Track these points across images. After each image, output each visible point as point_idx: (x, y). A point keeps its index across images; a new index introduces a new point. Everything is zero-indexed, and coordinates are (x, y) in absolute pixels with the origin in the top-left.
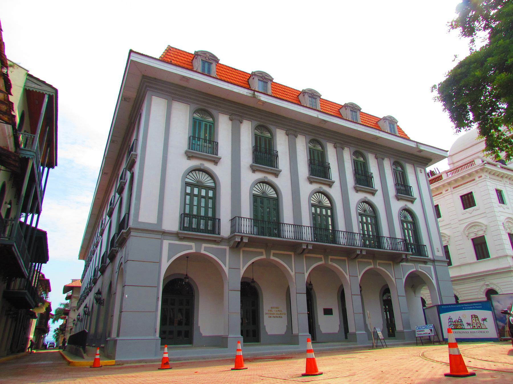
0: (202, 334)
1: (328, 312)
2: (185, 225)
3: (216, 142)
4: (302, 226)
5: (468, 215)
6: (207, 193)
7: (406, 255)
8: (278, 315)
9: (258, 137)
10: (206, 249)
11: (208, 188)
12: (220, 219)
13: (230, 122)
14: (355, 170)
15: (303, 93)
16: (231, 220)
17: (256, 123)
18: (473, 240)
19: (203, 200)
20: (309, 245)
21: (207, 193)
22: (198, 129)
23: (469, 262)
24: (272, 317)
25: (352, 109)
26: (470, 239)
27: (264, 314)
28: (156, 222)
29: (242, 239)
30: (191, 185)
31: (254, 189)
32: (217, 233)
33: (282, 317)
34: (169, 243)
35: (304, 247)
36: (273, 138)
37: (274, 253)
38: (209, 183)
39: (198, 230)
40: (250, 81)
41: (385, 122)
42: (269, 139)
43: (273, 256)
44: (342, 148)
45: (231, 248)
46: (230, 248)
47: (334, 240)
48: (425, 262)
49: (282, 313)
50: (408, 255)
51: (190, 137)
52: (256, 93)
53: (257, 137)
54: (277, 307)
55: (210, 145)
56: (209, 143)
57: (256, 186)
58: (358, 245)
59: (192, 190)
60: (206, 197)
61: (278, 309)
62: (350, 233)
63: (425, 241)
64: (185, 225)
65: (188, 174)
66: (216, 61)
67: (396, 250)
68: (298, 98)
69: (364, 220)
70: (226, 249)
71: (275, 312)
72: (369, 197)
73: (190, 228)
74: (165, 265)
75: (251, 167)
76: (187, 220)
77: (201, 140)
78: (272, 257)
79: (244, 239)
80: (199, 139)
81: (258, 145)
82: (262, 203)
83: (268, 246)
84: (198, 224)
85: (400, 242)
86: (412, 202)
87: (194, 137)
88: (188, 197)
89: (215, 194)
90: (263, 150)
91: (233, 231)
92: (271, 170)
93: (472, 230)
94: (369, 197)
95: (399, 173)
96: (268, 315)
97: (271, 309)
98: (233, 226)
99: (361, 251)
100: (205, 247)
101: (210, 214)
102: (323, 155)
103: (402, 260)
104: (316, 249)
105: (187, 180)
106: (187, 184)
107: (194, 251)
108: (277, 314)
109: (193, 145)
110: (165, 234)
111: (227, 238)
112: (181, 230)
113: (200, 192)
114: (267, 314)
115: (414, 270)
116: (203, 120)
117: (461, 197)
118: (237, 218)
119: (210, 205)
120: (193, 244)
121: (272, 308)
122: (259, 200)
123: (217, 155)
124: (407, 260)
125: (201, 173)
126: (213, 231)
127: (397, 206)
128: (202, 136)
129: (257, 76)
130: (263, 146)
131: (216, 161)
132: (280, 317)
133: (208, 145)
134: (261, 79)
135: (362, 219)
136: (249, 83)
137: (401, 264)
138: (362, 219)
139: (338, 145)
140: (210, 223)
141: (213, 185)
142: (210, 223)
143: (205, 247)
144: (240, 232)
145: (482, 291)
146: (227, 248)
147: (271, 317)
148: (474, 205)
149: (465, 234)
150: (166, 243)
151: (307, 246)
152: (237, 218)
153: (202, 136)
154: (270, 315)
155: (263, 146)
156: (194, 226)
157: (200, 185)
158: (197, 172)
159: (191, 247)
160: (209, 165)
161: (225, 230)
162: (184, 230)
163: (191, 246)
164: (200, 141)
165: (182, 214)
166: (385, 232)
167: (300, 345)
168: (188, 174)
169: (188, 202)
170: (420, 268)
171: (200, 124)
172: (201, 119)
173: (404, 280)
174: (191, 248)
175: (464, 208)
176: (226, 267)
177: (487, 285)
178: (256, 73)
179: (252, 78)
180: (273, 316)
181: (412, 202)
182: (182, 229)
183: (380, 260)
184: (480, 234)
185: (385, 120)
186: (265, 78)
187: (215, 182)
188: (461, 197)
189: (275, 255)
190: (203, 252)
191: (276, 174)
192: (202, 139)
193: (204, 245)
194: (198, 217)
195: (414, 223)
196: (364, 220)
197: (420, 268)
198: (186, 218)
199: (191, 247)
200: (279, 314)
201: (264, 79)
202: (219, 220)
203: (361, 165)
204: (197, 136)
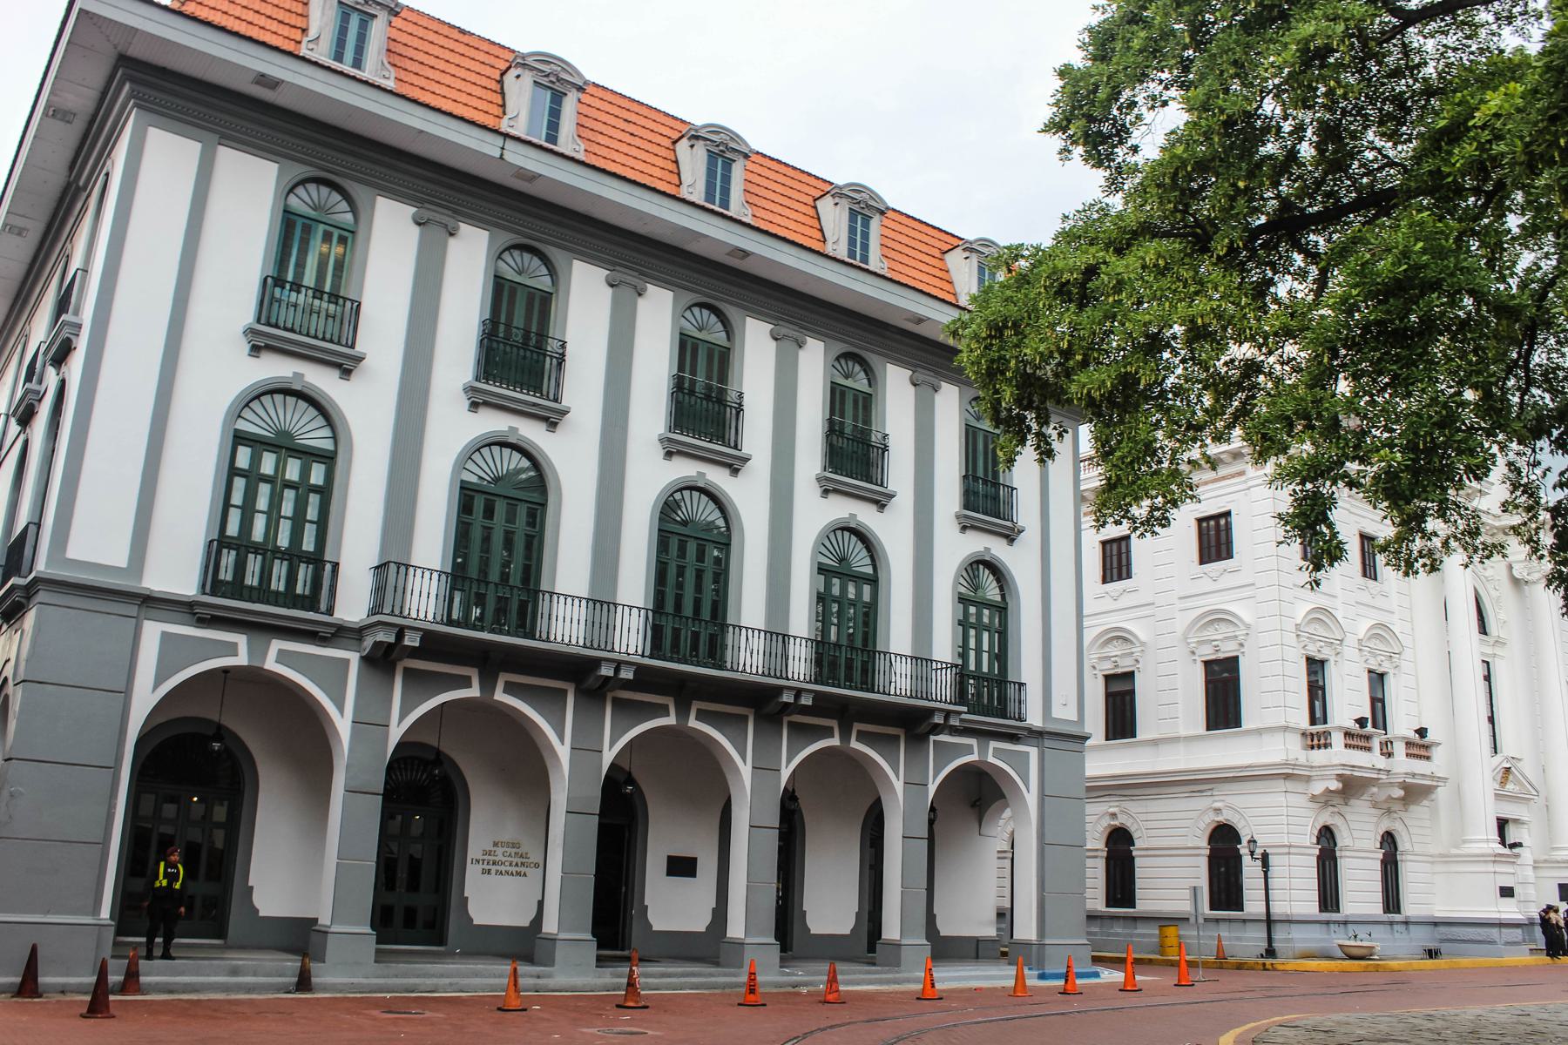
0: (258, 911)
1: (682, 867)
2: (222, 576)
3: (353, 301)
4: (615, 604)
5: (1207, 584)
6: (305, 472)
7: (948, 714)
8: (514, 869)
9: (507, 285)
10: (283, 657)
11: (310, 455)
12: (338, 564)
13: (415, 231)
14: (831, 422)
15: (689, 139)
16: (377, 568)
17: (507, 238)
18: (1207, 663)
19: (289, 495)
20: (623, 666)
21: (305, 472)
22: (299, 250)
23: (1183, 732)
24: (493, 872)
25: (856, 207)
26: (1199, 660)
27: (469, 861)
28: (124, 564)
29: (400, 635)
30: (251, 443)
31: (470, 465)
32: (323, 607)
33: (525, 875)
34: (165, 635)
35: (606, 671)
36: (557, 291)
37: (507, 683)
38: (315, 436)
39: (263, 593)
40: (509, 78)
41: (966, 258)
42: (544, 294)
43: (505, 691)
44: (796, 340)
45: (367, 660)
46: (362, 658)
48: (1013, 738)
49: (530, 861)
50: (952, 715)
51: (265, 280)
52: (510, 144)
53: (503, 285)
54: (513, 844)
55: (332, 307)
56: (329, 302)
57: (477, 457)
58: (790, 676)
59: (256, 460)
60: (303, 488)
61: (514, 850)
62: (777, 634)
63: (1027, 668)
64: (222, 576)
65: (239, 416)
66: (392, 9)
67: (922, 698)
68: (674, 151)
69: (836, 591)
70: (347, 662)
71: (504, 859)
72: (865, 515)
73: (237, 588)
75: (470, 390)
76: (229, 559)
77: (303, 290)
78: (500, 696)
79: (406, 637)
80: (297, 286)
81: (503, 319)
82: (489, 512)
83: (490, 661)
84: (266, 574)
85: (942, 669)
86: (1011, 540)
87: (279, 282)
88: (239, 484)
89: (329, 476)
90: (518, 336)
91: (376, 609)
92: (534, 405)
93: (1210, 633)
94: (865, 515)
96: (480, 867)
97: (493, 849)
98: (379, 590)
99: (799, 693)
100: (280, 651)
101: (308, 545)
102: (722, 360)
103: (936, 729)
104: (646, 679)
105: (242, 425)
106: (240, 438)
107: (245, 663)
108: (511, 865)
109: (276, 305)
111: (357, 626)
112: (204, 593)
113: (280, 467)
114: (478, 861)
115: (974, 757)
116: (319, 219)
117: (1200, 521)
118: (393, 567)
119: (312, 513)
120: (241, 640)
121: (496, 844)
122: (479, 504)
123: (353, 347)
124: (954, 731)
125: (291, 400)
126: (311, 602)
128: (309, 279)
129: (532, 69)
130: (519, 321)
131: (346, 366)
132: (518, 874)
133: (325, 305)
134: (544, 81)
135: (828, 585)
136: (502, 88)
137: (932, 738)
138: (828, 585)
139: (784, 331)
140: (304, 573)
141: (327, 445)
142: (304, 573)
143: (280, 651)
144: (397, 612)
145: (1202, 826)
146: (354, 658)
147: (489, 870)
148: (1230, 556)
149: (1189, 644)
150: (153, 632)
151: (617, 670)
152: (393, 567)
153: (309, 279)
154: (488, 867)
155: (519, 321)
156: (252, 580)
157: (284, 445)
158: (279, 398)
160: (321, 379)
161: (352, 605)
162: (213, 594)
163: (236, 644)
164: (299, 292)
165: (211, 541)
166: (898, 635)
167: (556, 967)
168: (247, 405)
169: (237, 498)
170: (993, 754)
171: (307, 230)
172: (312, 214)
173: (932, 789)
174: (232, 649)
175: (1202, 562)
176: (342, 716)
177: (1218, 811)
178: (530, 61)
179: (513, 72)
180: (497, 871)
181: (1011, 540)
182: (208, 589)
183: (860, 721)
184: (1227, 650)
185: (967, 254)
186: (559, 79)
187: (335, 438)
188: (1200, 521)
189: (510, 688)
190: (271, 664)
191: (552, 420)
192: (308, 288)
193: (276, 645)
194: (268, 551)
195: (1005, 609)
196: (836, 591)
197: (993, 754)
198: (225, 551)
200: (517, 865)
201: (553, 83)
202: (336, 566)
203: (856, 402)
204: (290, 277)
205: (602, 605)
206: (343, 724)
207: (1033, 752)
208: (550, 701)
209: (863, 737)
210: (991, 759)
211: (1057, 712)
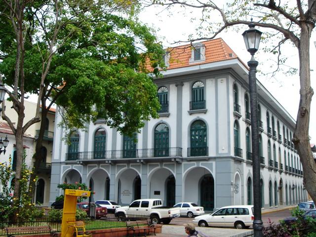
47: (134, 155)
74: (62, 175)
78: (100, 168)
95: (200, 90)
110: (61, 163)
115: (196, 166)
120: (70, 166)
127: (187, 120)
150: (62, 166)
159: (70, 167)
166: (173, 143)
174: (69, 167)
189: (102, 166)
190: (74, 168)
193: (74, 165)
199: (70, 167)
205: (114, 151)
206: (81, 175)
207: (214, 163)
208: (107, 167)
209: (165, 165)
210: (201, 166)
211: (220, 152)
